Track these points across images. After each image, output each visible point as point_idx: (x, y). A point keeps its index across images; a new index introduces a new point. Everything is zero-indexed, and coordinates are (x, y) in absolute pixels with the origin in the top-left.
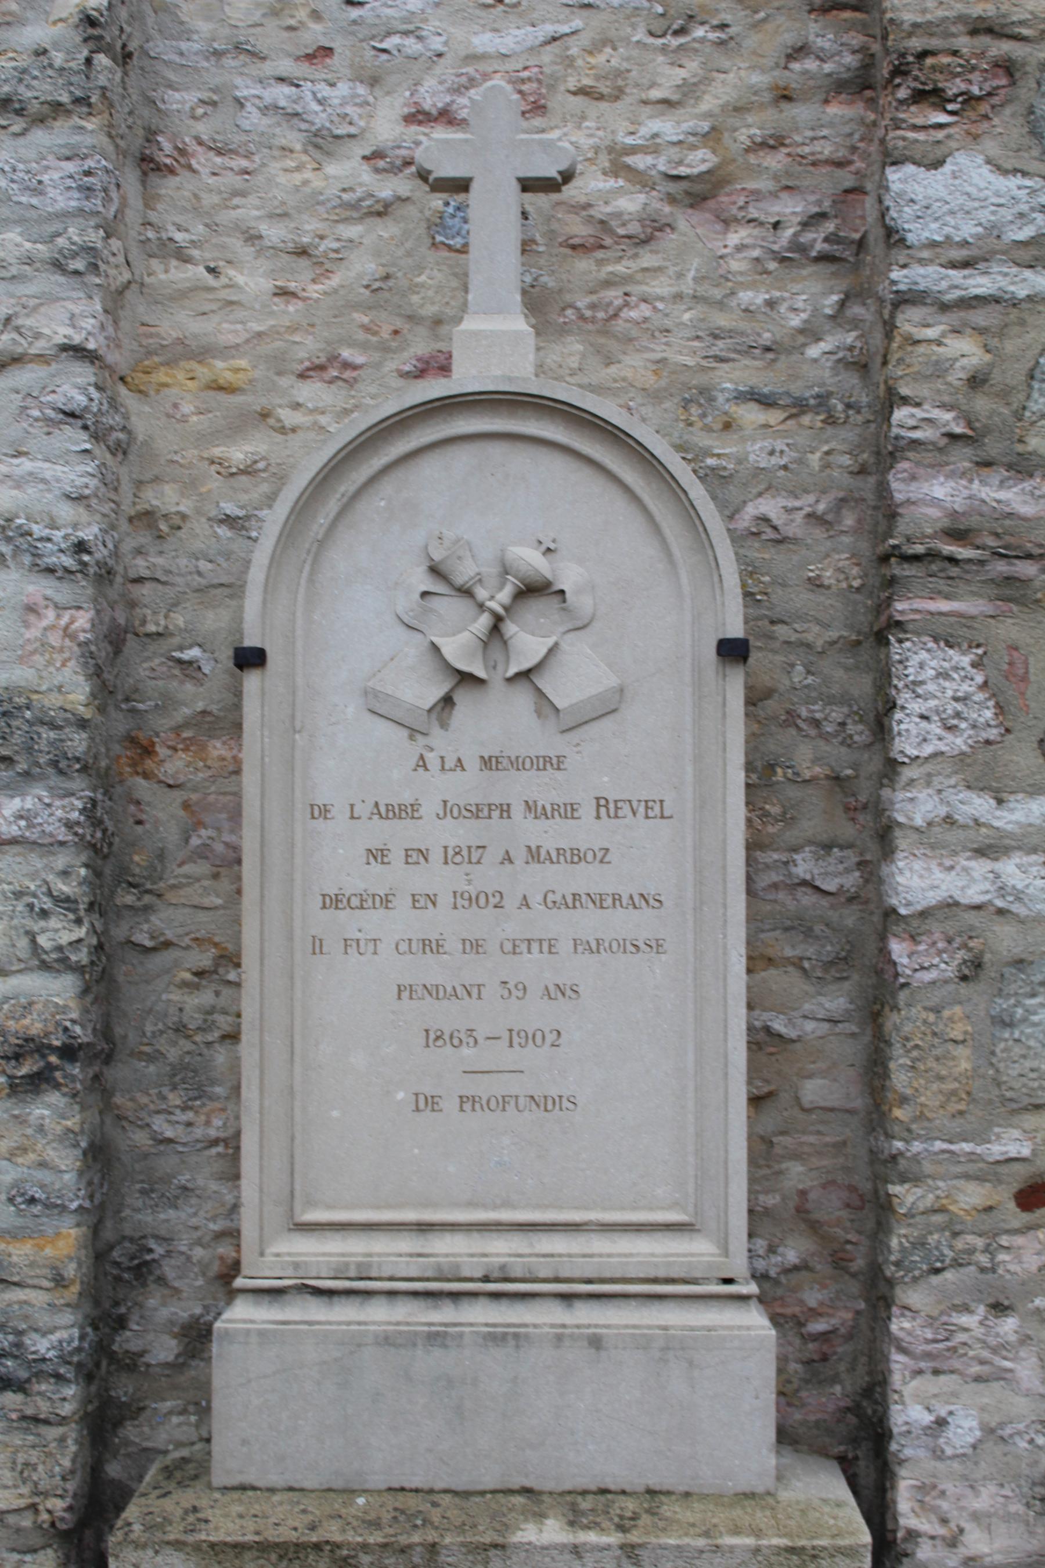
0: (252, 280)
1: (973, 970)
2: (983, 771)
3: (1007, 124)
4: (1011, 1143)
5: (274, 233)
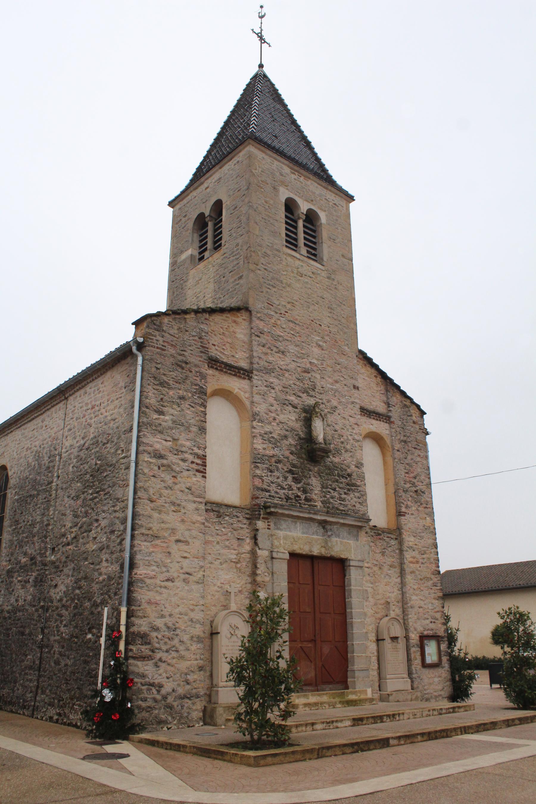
3: (264, 589)
5: (211, 593)
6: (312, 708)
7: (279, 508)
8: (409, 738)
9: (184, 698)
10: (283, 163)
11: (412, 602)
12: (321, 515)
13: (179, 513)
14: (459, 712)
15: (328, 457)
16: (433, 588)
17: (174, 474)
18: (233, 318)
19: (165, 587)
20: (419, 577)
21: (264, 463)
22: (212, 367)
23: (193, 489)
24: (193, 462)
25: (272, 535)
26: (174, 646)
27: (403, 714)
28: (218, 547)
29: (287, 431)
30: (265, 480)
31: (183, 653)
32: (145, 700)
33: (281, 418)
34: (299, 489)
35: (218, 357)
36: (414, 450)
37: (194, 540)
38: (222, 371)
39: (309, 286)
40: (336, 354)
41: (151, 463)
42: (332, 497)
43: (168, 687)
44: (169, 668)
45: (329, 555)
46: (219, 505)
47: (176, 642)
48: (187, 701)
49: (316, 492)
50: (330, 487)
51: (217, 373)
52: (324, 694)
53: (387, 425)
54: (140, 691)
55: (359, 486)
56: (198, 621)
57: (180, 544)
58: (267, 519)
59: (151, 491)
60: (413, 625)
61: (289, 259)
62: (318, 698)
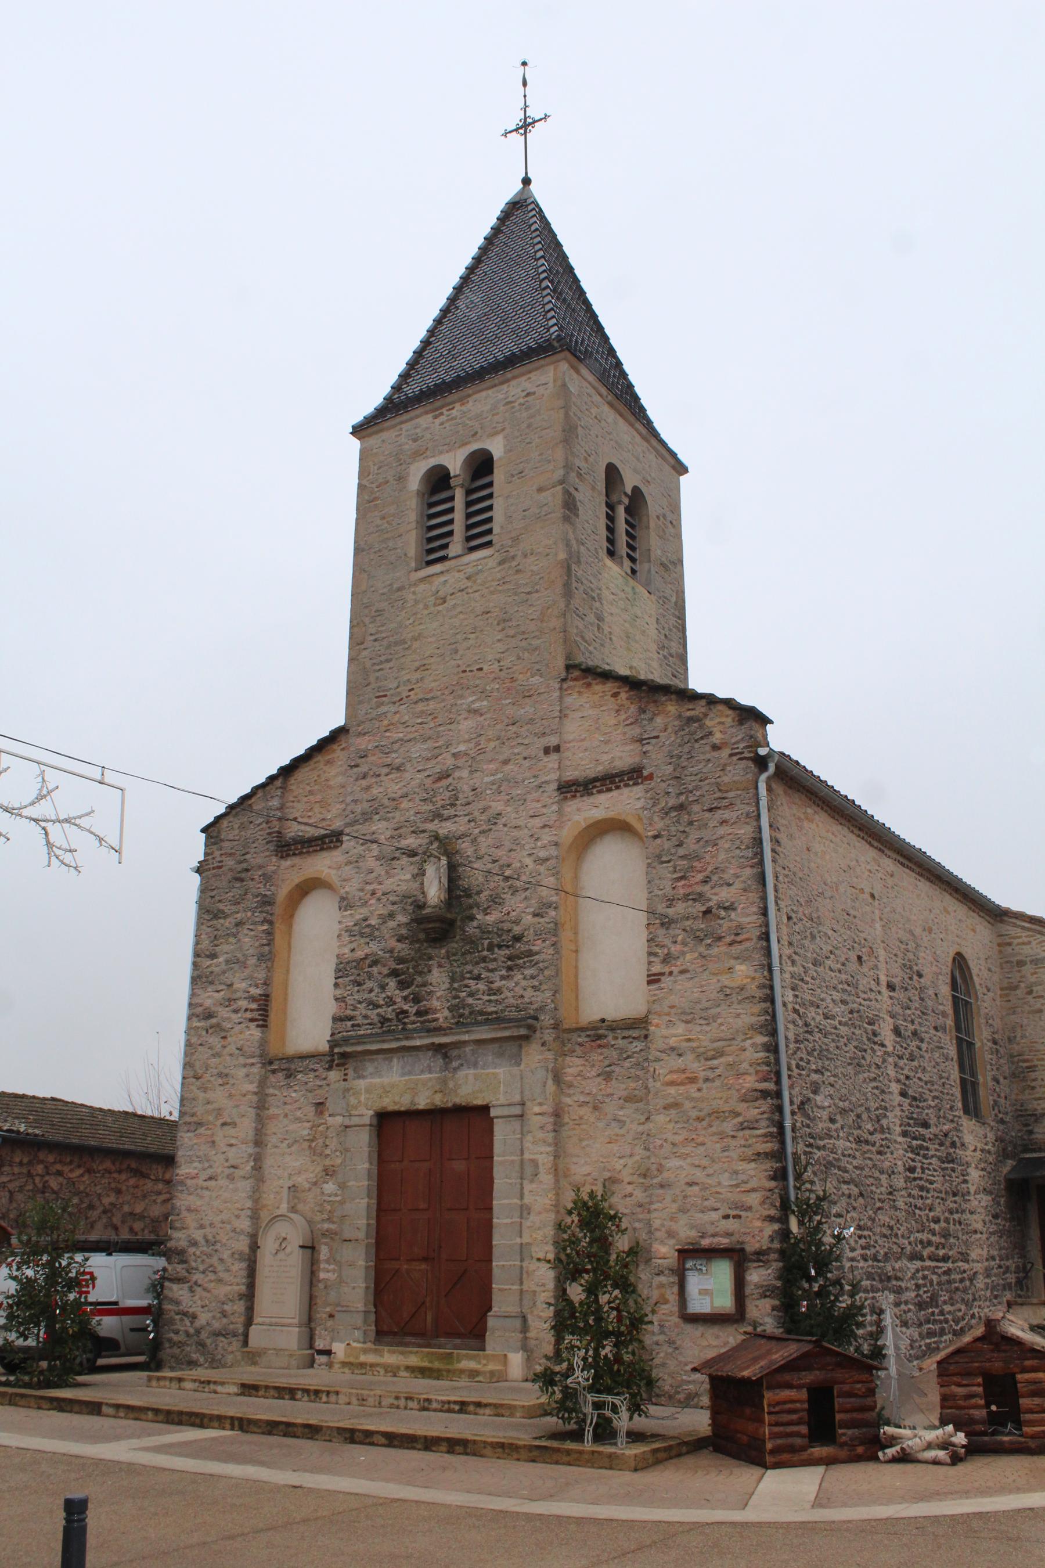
0: (272, 1196)
1: (325, 1287)
2: (328, 1262)
4: (328, 1309)
6: (356, 1371)
7: (346, 1045)
8: (353, 1436)
9: (218, 1335)
10: (417, 417)
11: (665, 1175)
12: (420, 1037)
13: (227, 1086)
14: (476, 1414)
15: (472, 918)
16: (740, 1134)
17: (223, 1034)
18: (327, 758)
19: (207, 1188)
20: (694, 1114)
21: (347, 975)
22: (288, 855)
23: (246, 1048)
24: (246, 1010)
25: (348, 1090)
26: (211, 1266)
27: (337, 1393)
28: (286, 1121)
29: (394, 903)
30: (350, 1002)
31: (221, 1275)
32: (177, 1332)
33: (389, 884)
34: (405, 998)
35: (300, 834)
36: (707, 815)
37: (244, 1119)
38: (301, 853)
39: (459, 609)
40: (510, 706)
41: (198, 1028)
42: (471, 995)
43: (203, 1318)
44: (205, 1294)
45: (450, 1105)
46: (290, 1059)
47: (214, 1260)
48: (223, 1339)
49: (438, 994)
50: (468, 975)
51: (296, 860)
52: (411, 1352)
53: (638, 790)
54: (172, 1322)
55: (537, 953)
56: (242, 1232)
57: (226, 1128)
58: (343, 1065)
59: (198, 1064)
60: (663, 1225)
61: (422, 587)
62: (401, 1357)
